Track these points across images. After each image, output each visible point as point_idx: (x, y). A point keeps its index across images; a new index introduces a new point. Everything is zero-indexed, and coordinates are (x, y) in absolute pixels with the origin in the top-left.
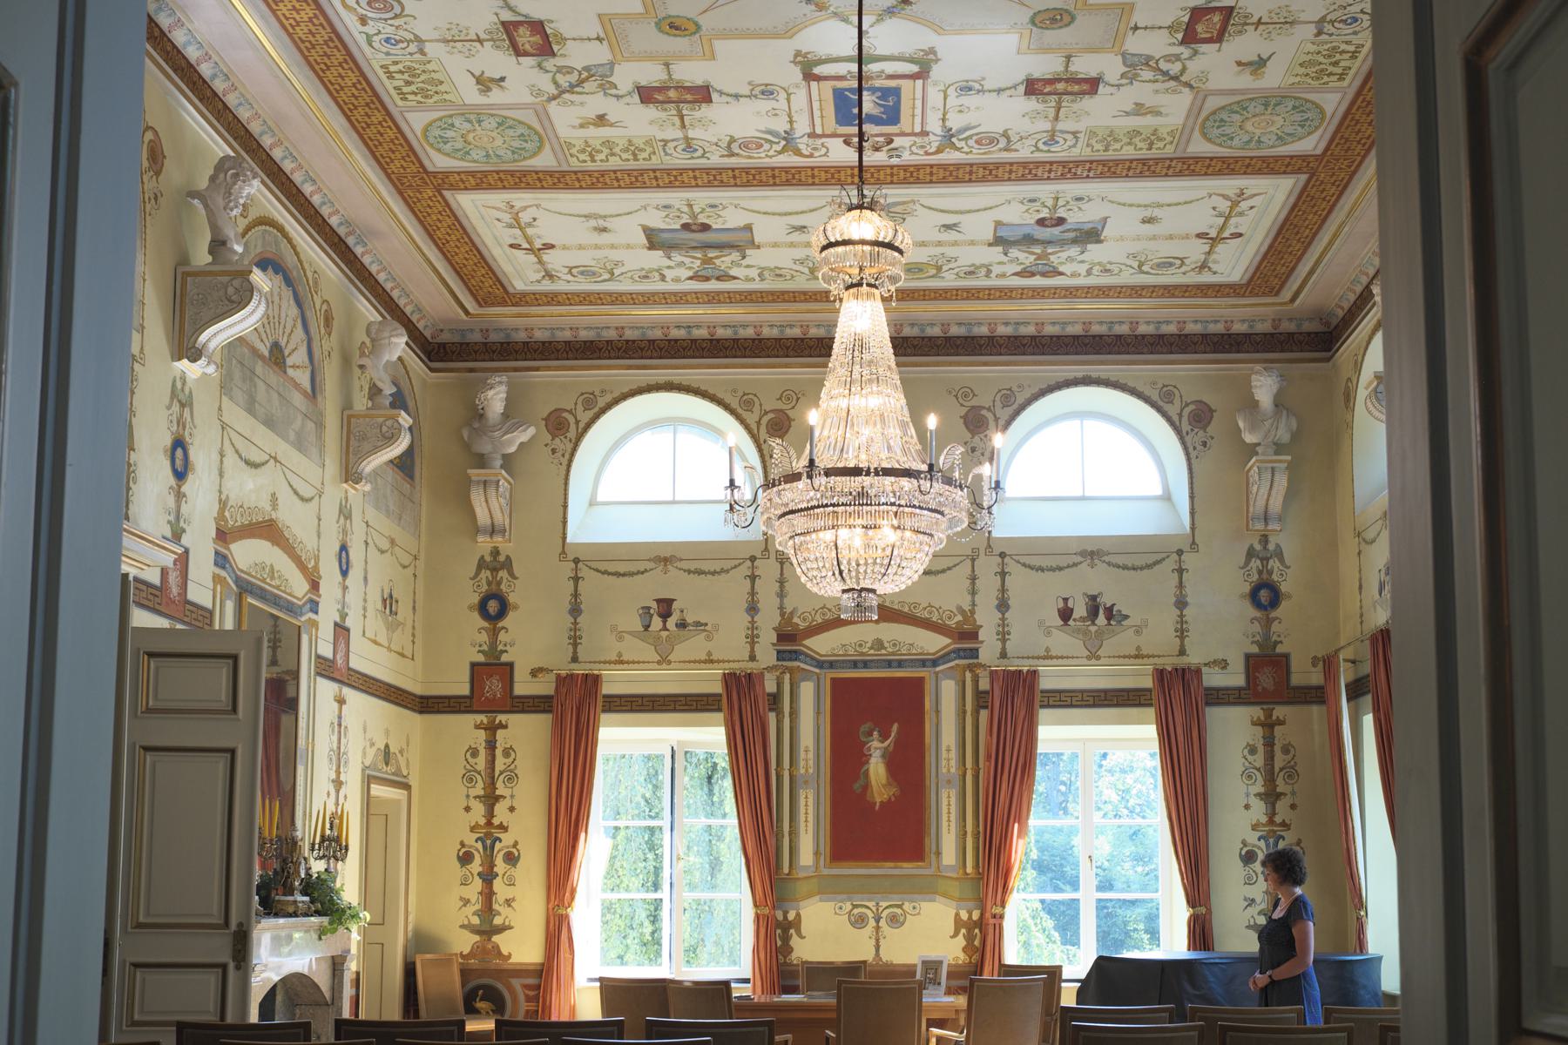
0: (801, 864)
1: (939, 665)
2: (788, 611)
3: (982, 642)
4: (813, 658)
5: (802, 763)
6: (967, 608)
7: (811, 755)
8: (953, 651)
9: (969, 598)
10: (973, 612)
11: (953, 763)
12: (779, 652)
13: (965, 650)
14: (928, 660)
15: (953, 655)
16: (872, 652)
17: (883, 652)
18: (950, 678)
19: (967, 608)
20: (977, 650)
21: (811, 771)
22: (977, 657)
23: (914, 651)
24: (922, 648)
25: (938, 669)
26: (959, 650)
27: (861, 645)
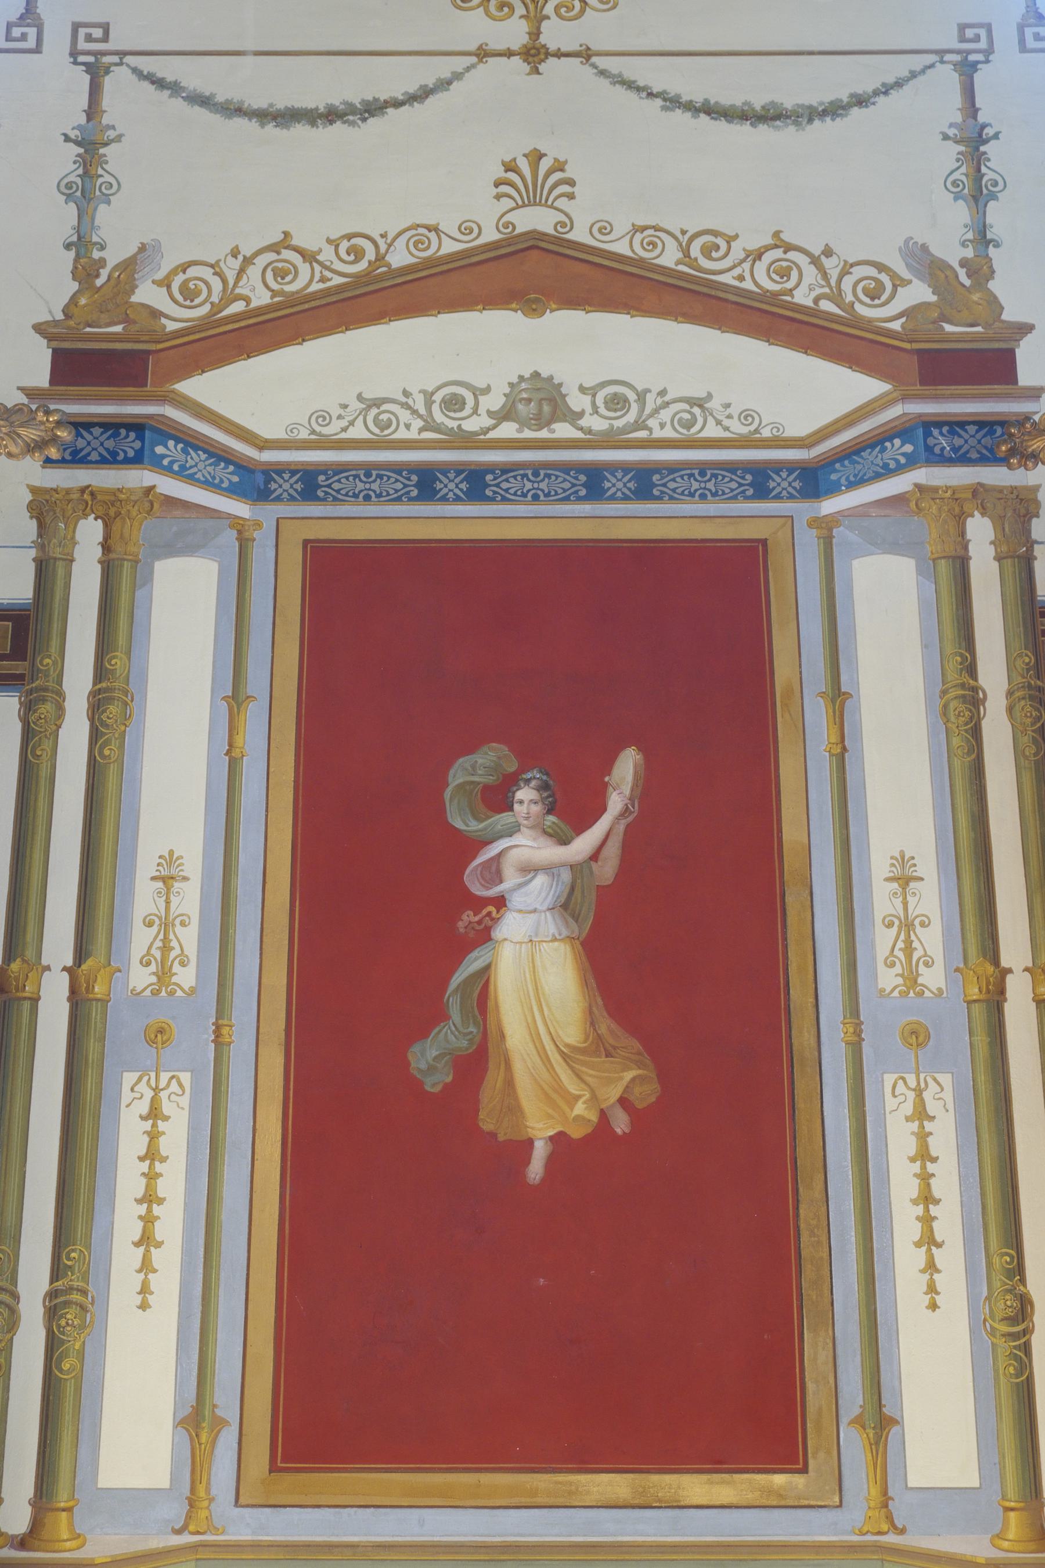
0: (106, 1479)
1: (834, 489)
2: (114, 256)
8: (902, 431)
9: (961, 213)
13: (955, 425)
14: (778, 467)
15: (899, 448)
16: (508, 430)
17: (563, 430)
18: (895, 548)
21: (185, 977)
23: (711, 431)
24: (746, 416)
25: (829, 506)
26: (929, 424)
27: (454, 403)
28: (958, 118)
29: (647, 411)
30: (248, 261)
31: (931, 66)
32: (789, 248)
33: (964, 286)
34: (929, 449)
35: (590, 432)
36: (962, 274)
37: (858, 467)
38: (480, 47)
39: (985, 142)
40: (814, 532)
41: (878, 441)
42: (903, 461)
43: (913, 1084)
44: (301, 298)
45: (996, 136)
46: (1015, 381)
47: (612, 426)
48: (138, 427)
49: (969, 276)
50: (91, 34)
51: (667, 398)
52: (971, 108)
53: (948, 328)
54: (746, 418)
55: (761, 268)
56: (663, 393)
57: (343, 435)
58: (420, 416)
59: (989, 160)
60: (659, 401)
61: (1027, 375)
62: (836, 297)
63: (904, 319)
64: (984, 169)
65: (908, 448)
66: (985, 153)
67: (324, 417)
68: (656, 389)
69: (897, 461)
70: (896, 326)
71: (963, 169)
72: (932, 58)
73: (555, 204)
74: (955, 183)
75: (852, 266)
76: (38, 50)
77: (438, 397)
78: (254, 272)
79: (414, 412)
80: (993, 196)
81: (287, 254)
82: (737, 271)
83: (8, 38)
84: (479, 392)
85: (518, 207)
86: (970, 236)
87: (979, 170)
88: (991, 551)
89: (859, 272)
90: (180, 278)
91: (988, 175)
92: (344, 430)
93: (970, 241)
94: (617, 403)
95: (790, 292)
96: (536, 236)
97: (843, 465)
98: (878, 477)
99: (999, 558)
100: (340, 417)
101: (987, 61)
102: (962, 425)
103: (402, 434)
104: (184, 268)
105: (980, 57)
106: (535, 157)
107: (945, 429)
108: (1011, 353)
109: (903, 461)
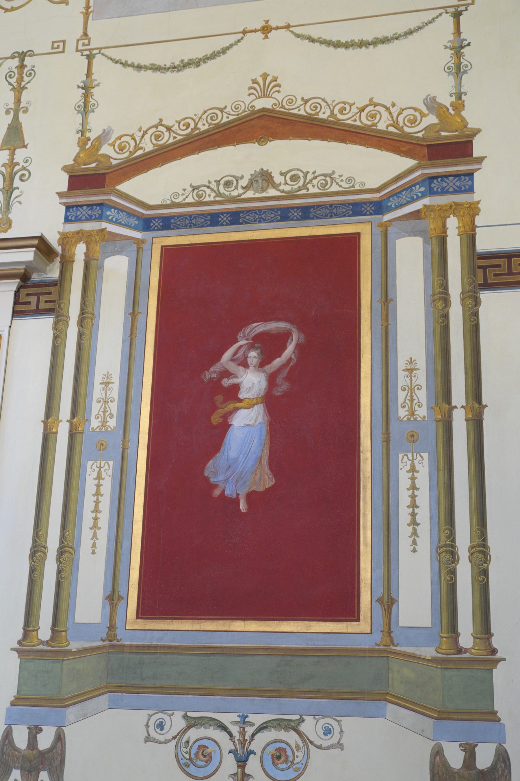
1: (390, 210)
2: (92, 136)
3: (480, 160)
4: (131, 214)
5: (96, 408)
7: (115, 392)
9: (451, 80)
11: (422, 395)
12: (68, 208)
15: (419, 189)
16: (250, 194)
20: (470, 175)
23: (335, 188)
24: (350, 180)
25: (387, 217)
26: (432, 178)
27: (228, 184)
28: (452, 37)
29: (307, 181)
30: (145, 133)
31: (440, 15)
32: (376, 105)
33: (451, 114)
35: (283, 191)
36: (450, 109)
37: (400, 199)
38: (244, 30)
40: (380, 229)
42: (420, 195)
43: (410, 458)
44: (162, 147)
45: (469, 44)
46: (471, 155)
47: (292, 188)
48: (101, 205)
50: (84, 43)
51: (316, 175)
52: (458, 31)
53: (443, 134)
54: (349, 181)
55: (364, 115)
56: (314, 173)
57: (184, 202)
58: (215, 191)
59: (464, 56)
60: (313, 176)
62: (395, 124)
63: (424, 132)
64: (462, 60)
65: (423, 189)
66: (463, 53)
67: (176, 194)
68: (311, 172)
69: (417, 195)
70: (420, 135)
73: (272, 96)
75: (403, 110)
76: (63, 52)
77: (222, 182)
78: (147, 137)
79: (212, 190)
80: (465, 72)
81: (160, 128)
82: (353, 119)
83: (53, 48)
84: (237, 179)
85: (257, 98)
86: (454, 91)
87: (460, 61)
89: (405, 113)
90: (118, 142)
92: (184, 199)
93: (454, 93)
94: (295, 178)
95: (375, 125)
96: (264, 110)
98: (408, 203)
100: (183, 194)
101: (467, 10)
103: (207, 199)
104: (120, 138)
105: (463, 8)
106: (265, 76)
108: (471, 142)
109: (420, 195)
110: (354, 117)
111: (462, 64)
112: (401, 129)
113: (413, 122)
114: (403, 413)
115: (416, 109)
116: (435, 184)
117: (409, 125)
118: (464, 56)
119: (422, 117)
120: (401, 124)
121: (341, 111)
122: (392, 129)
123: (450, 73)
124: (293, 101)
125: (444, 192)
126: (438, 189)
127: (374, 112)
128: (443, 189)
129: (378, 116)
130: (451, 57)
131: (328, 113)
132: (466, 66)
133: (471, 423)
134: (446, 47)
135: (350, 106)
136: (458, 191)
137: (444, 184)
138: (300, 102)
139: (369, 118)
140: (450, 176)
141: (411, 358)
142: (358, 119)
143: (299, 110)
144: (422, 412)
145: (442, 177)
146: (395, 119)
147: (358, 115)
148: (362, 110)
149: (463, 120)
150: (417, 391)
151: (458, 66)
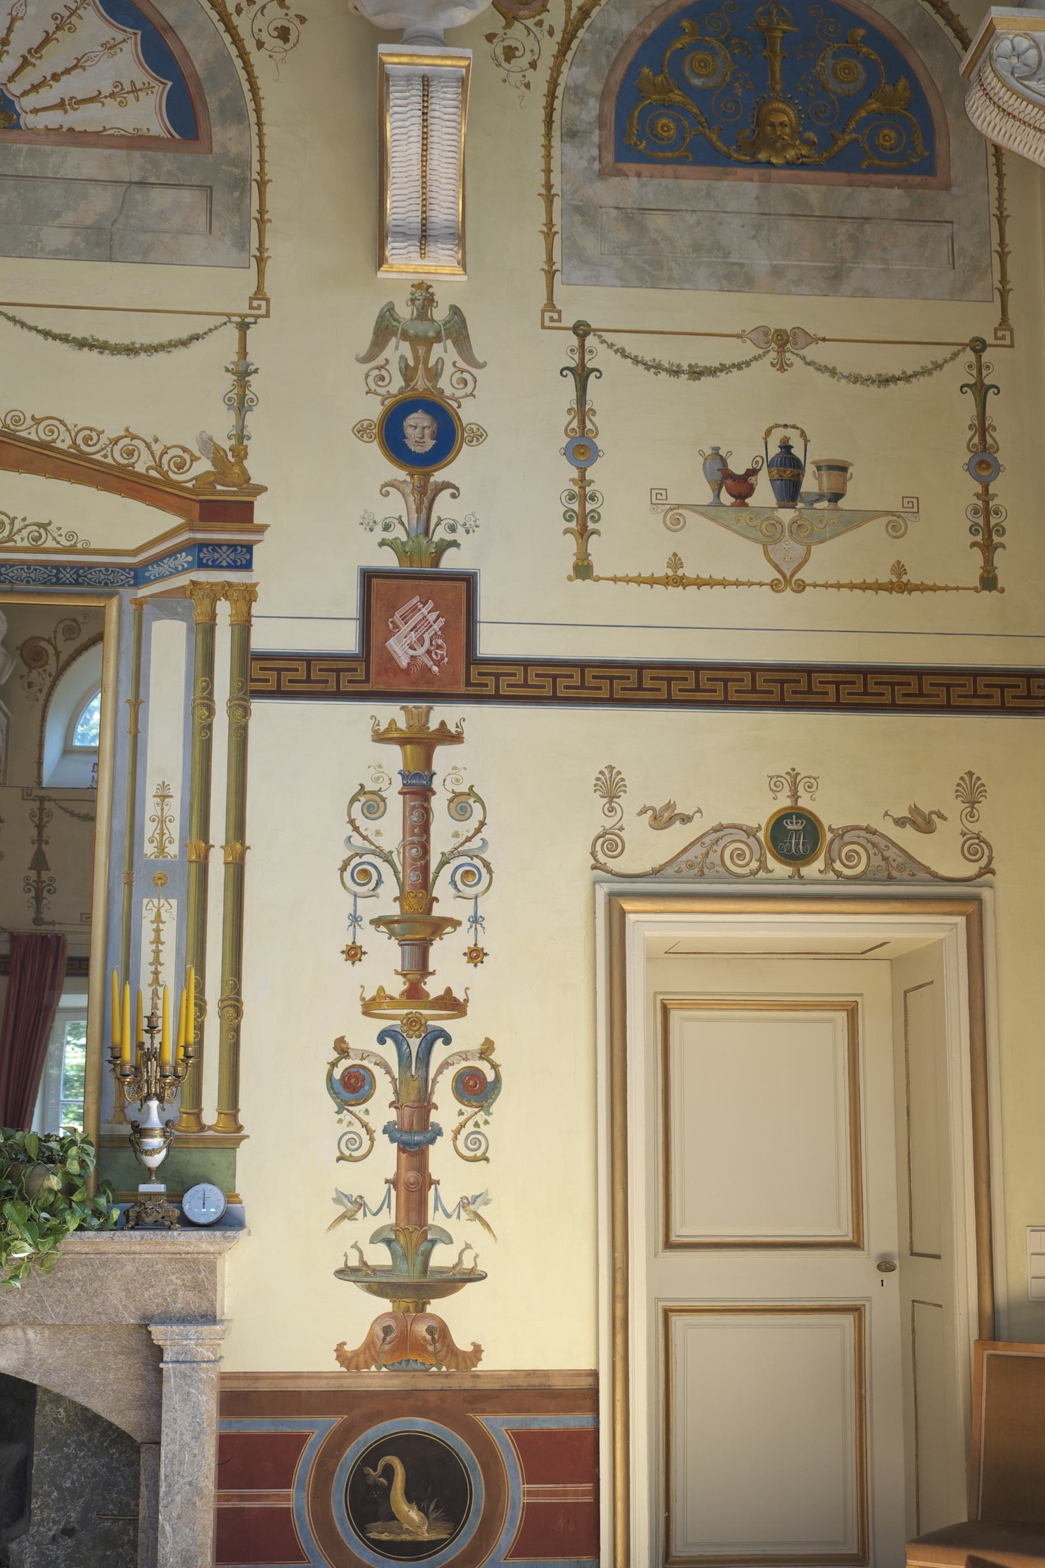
1: (148, 581)
3: (262, 529)
6: (226, 444)
10: (241, 453)
11: (174, 829)
13: (216, 546)
15: (185, 558)
19: (226, 444)
20: (249, 548)
22: (248, 566)
25: (143, 592)
26: (202, 545)
28: (235, 358)
34: (200, 560)
36: (230, 454)
39: (249, 374)
40: (134, 606)
41: (172, 553)
42: (186, 565)
49: (233, 457)
52: (243, 352)
53: (219, 487)
59: (250, 386)
61: (259, 518)
62: (159, 467)
63: (194, 482)
64: (247, 392)
65: (190, 558)
66: (248, 381)
70: (190, 485)
71: (236, 391)
72: (225, 319)
74: (230, 400)
75: (168, 449)
86: (234, 432)
88: (228, 620)
91: (249, 395)
97: (153, 567)
99: (232, 625)
101: (255, 323)
102: (220, 546)
107: (210, 548)
108: (252, 503)
109: (186, 565)
110: (104, 452)
111: (247, 397)
112: (165, 475)
113: (180, 466)
114: (149, 849)
115: (185, 450)
116: (205, 555)
117: (176, 470)
118: (250, 386)
119: (192, 461)
120: (166, 468)
121: (86, 440)
122: (153, 473)
123: (230, 407)
124: (20, 420)
125: (216, 566)
126: (208, 560)
127: (130, 448)
128: (214, 561)
129: (136, 454)
130: (233, 385)
131: (69, 442)
132: (252, 401)
133: (231, 867)
134: (227, 370)
135: (98, 435)
136: (232, 567)
137: (216, 556)
138: (29, 422)
139: (125, 456)
140: (223, 545)
141: (164, 782)
142: (109, 454)
143: (30, 433)
144: (173, 849)
145: (213, 545)
146: (157, 459)
147: (109, 449)
148: (115, 442)
149: (244, 472)
150: (168, 823)
151: (242, 397)
